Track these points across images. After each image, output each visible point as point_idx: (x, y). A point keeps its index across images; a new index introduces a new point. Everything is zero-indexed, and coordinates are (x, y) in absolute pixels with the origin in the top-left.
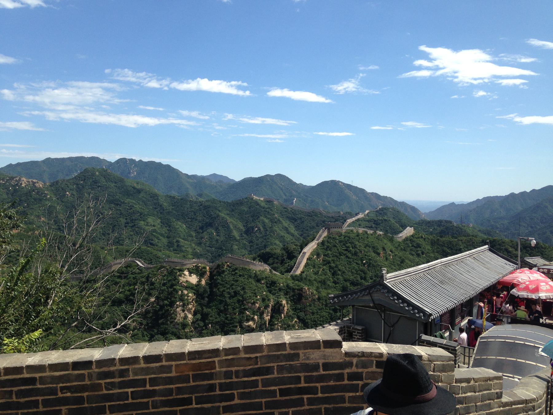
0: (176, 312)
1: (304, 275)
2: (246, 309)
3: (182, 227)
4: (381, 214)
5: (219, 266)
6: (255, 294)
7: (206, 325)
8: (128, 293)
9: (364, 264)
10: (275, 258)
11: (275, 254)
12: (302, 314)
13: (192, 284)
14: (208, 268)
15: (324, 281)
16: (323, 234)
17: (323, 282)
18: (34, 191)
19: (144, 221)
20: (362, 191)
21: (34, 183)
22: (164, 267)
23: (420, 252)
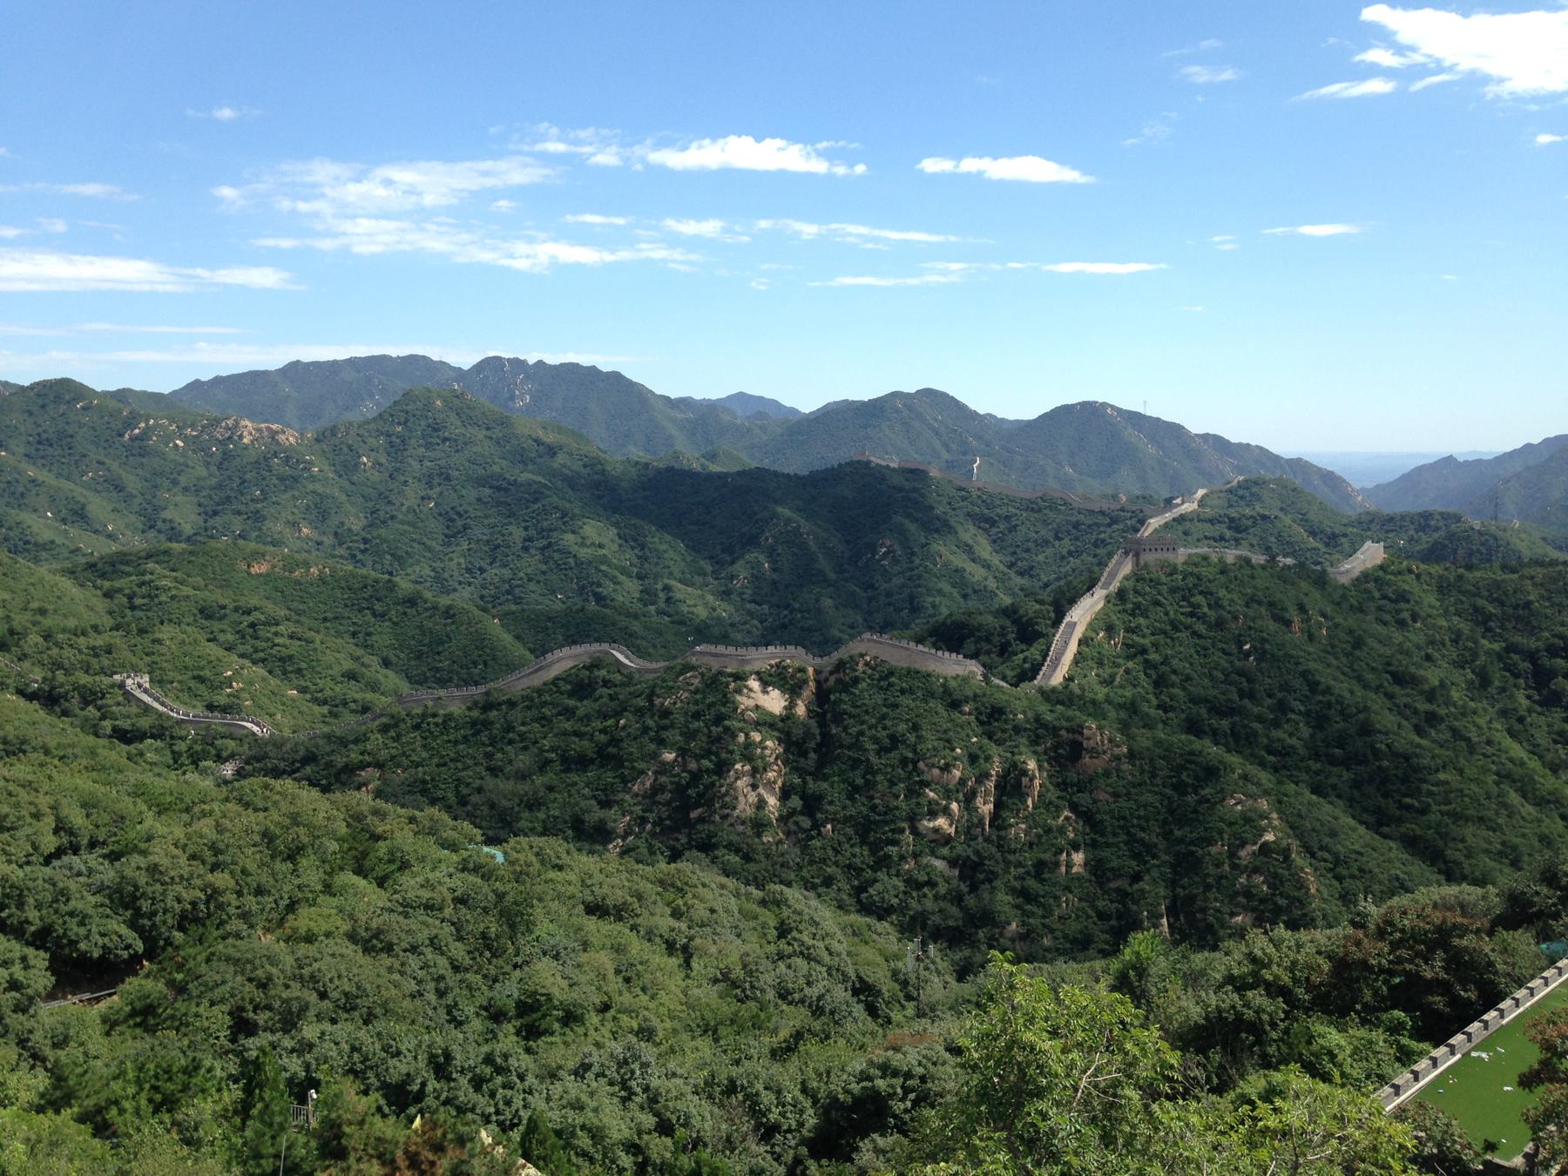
0: (735, 790)
1: (1074, 686)
2: (927, 784)
4: (1242, 497)
5: (840, 666)
6: (948, 741)
7: (817, 826)
8: (603, 738)
9: (1248, 654)
10: (980, 638)
11: (980, 627)
12: (1083, 799)
13: (771, 715)
14: (811, 670)
15: (1133, 703)
16: (1122, 569)
17: (1132, 708)
18: (275, 455)
20: (1176, 430)
21: (273, 434)
22: (693, 668)
23: (1406, 615)
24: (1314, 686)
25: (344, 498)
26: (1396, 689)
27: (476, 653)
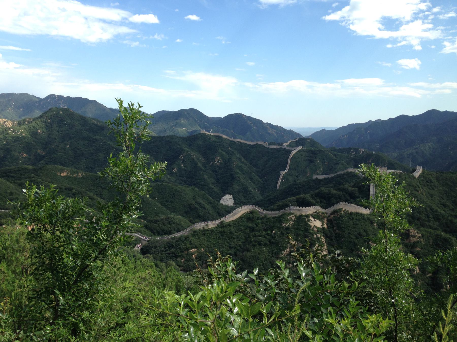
3: (152, 160)
20: (260, 122)
23: (433, 187)
24: (432, 209)
25: (35, 144)
26: (446, 210)
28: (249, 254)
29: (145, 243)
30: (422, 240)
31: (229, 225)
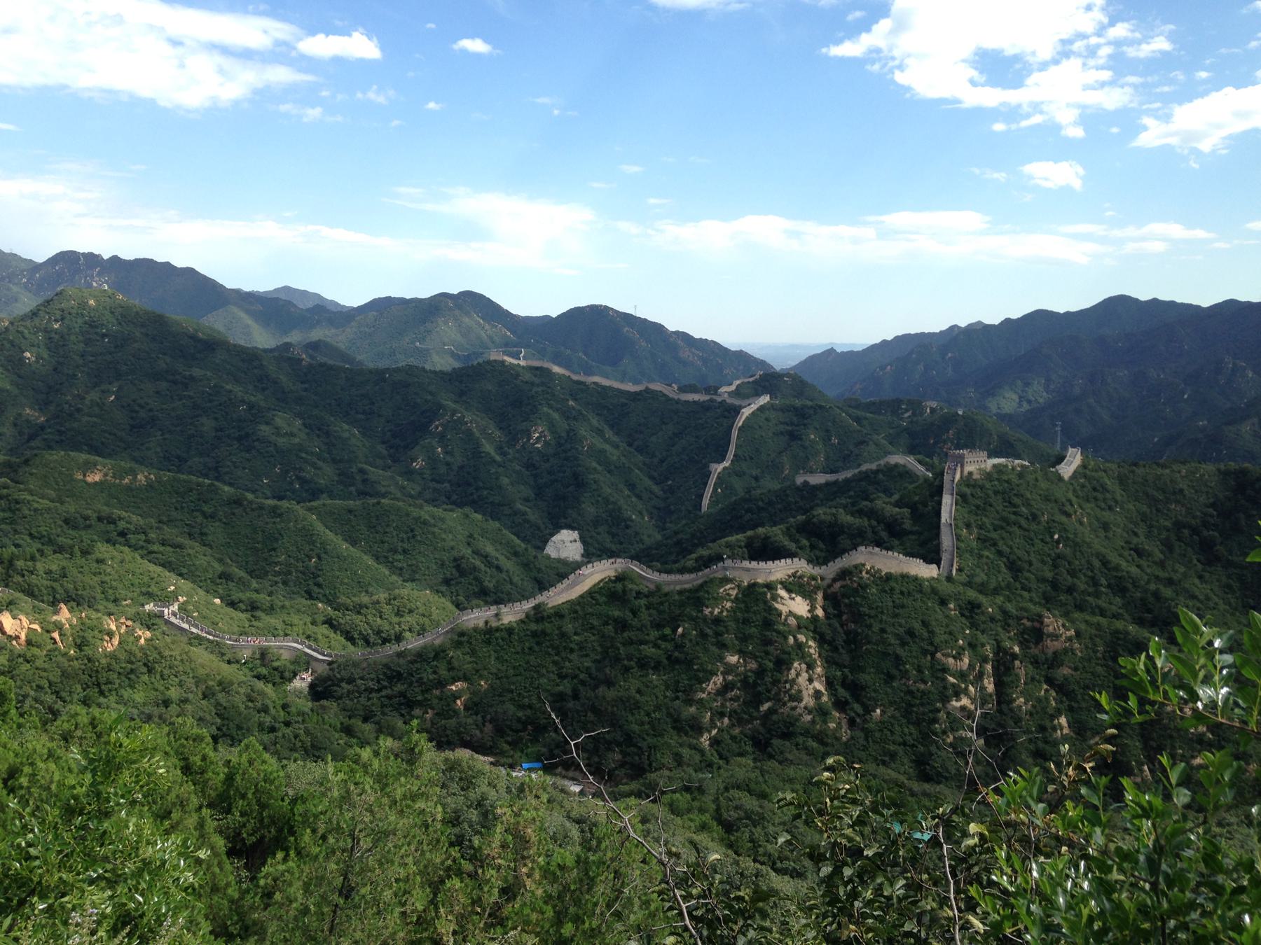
3: (354, 435)
9: (1058, 542)
19: (267, 423)
20: (658, 328)
24: (1105, 563)
25: (16, 391)
26: (1144, 563)
27: (307, 548)
28: (611, 694)
29: (322, 669)
30: (1077, 645)
31: (558, 613)
